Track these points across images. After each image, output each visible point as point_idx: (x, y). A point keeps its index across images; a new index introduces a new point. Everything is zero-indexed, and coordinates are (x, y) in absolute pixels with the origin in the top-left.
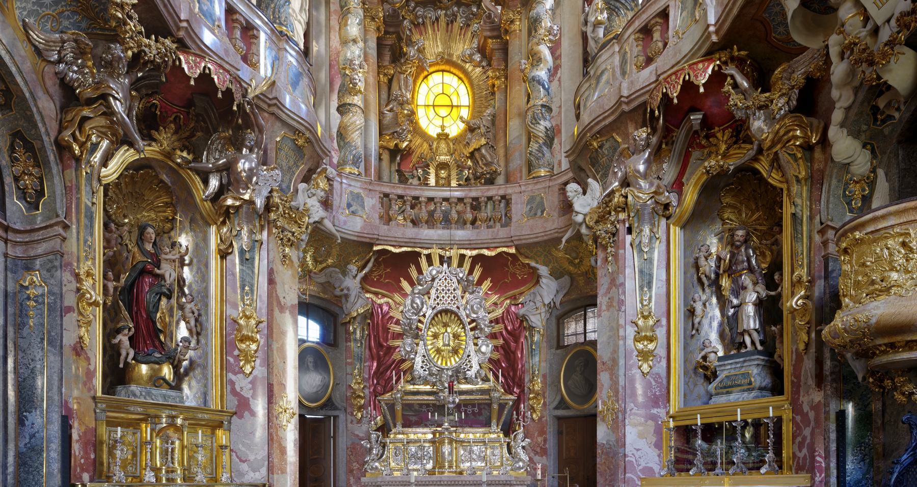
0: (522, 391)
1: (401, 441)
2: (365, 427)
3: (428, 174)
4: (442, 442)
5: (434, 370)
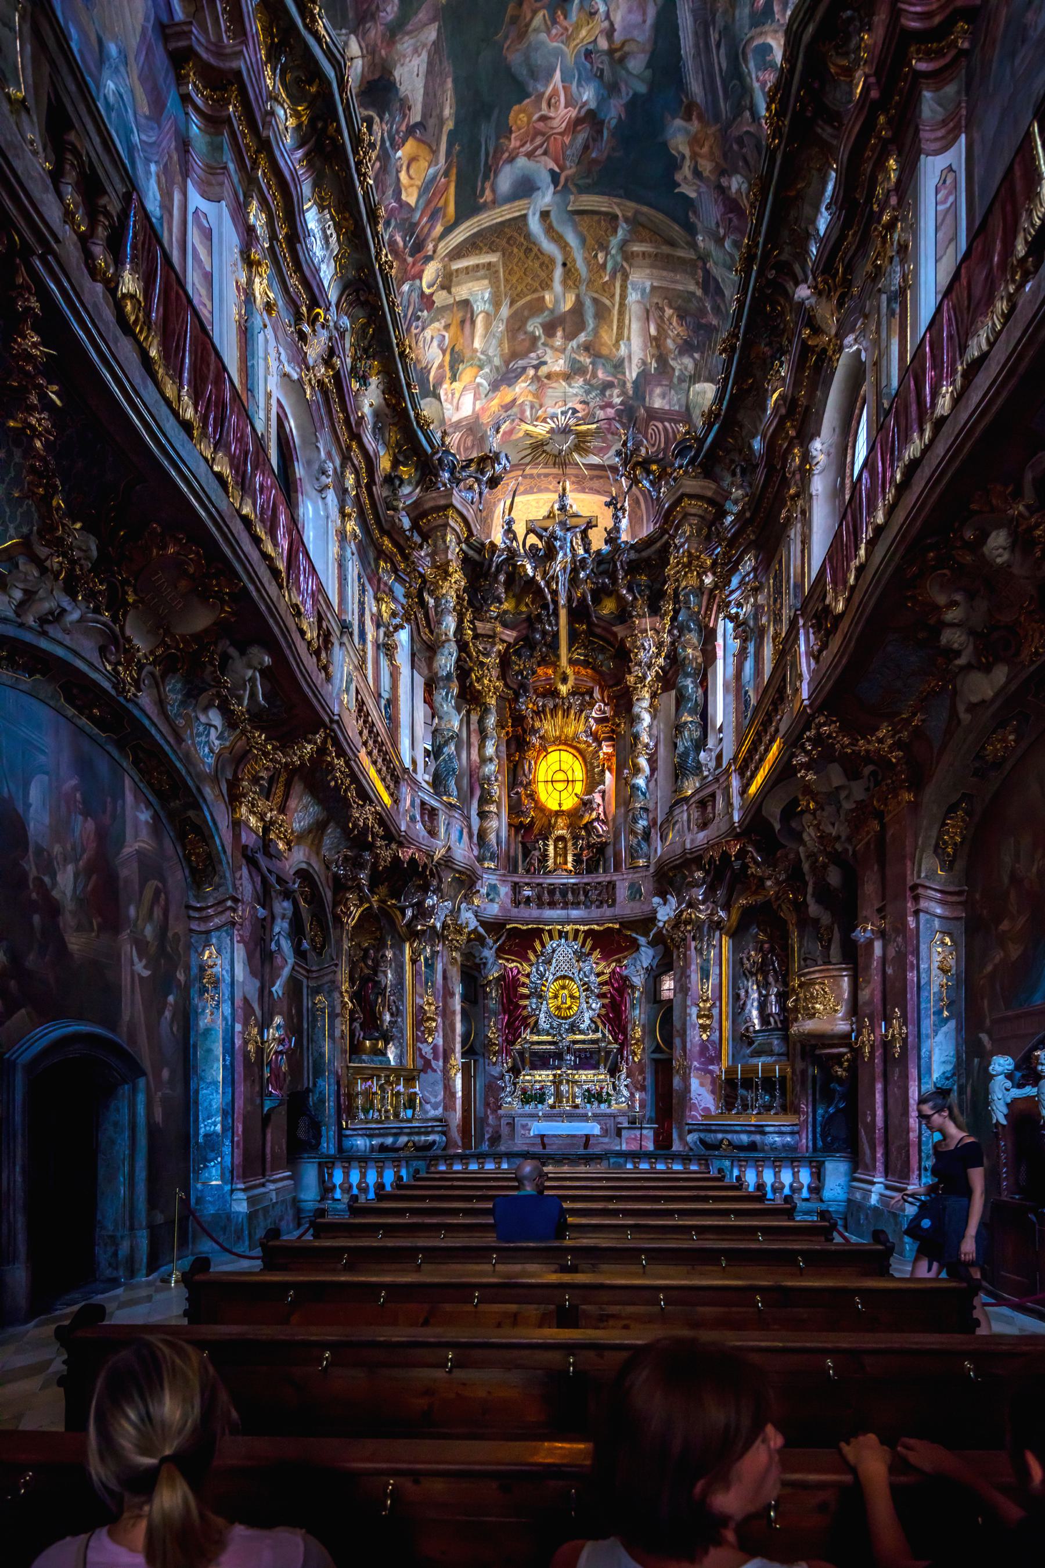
2: (498, 1069)
4: (561, 1082)
5: (555, 1024)
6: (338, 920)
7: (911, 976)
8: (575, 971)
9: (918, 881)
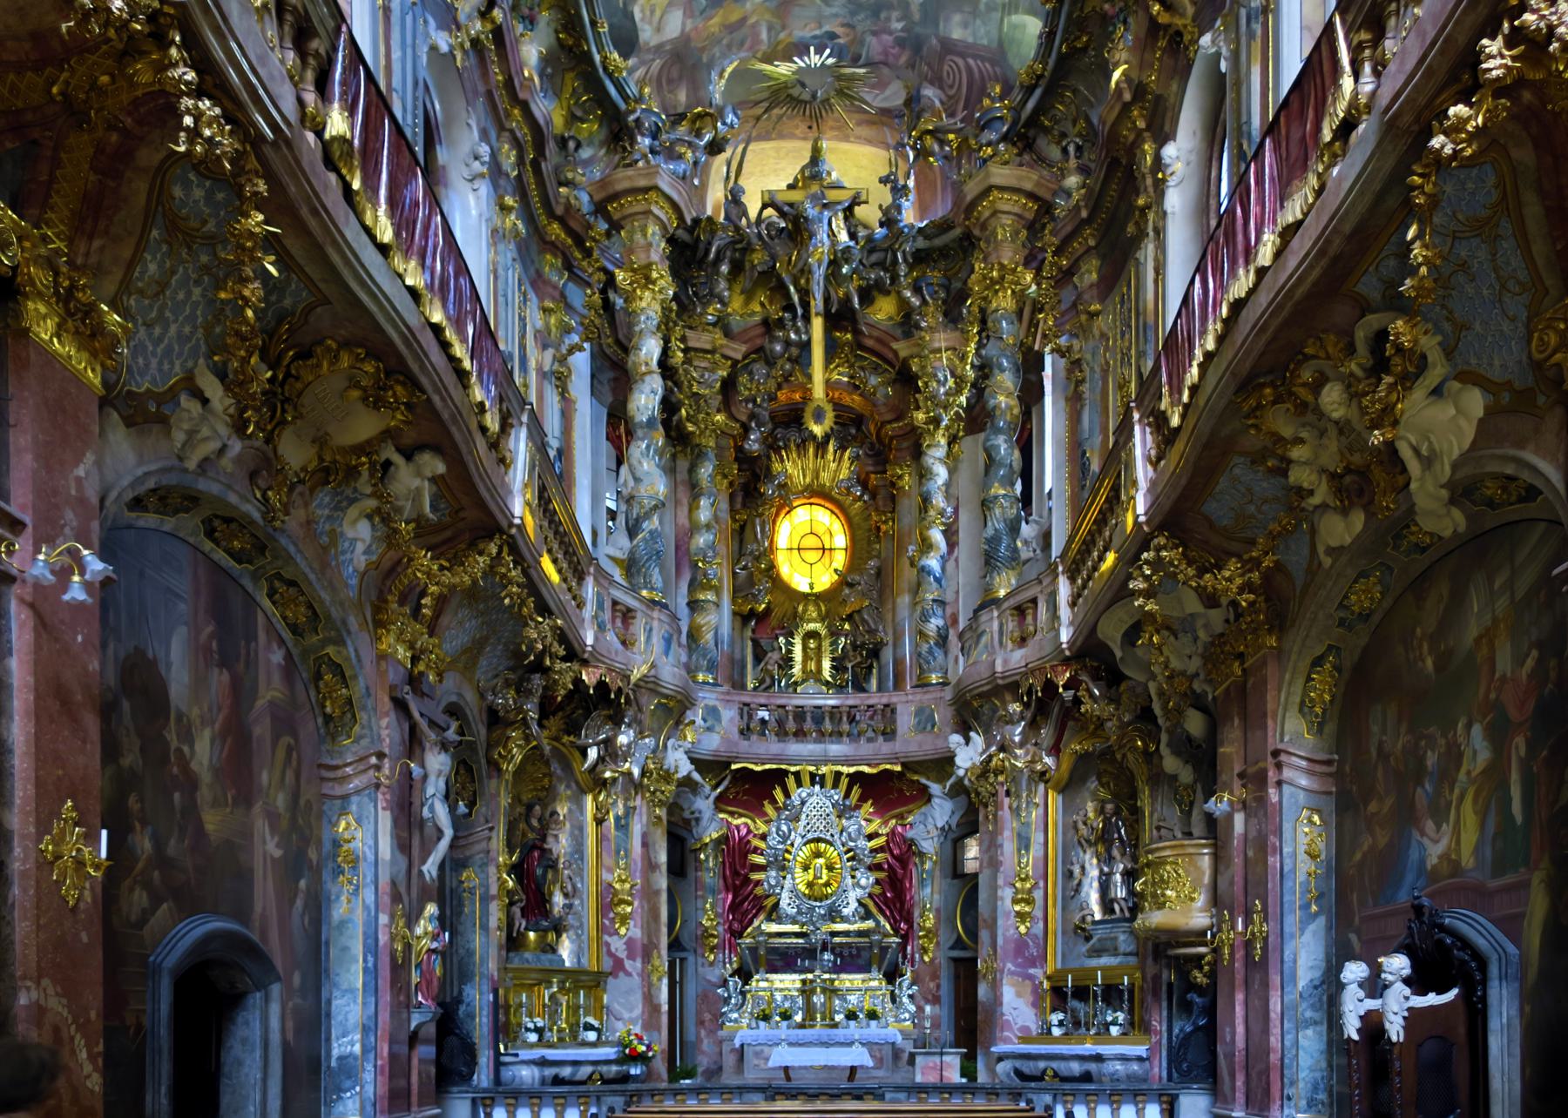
0: (911, 926)
1: (764, 990)
3: (792, 644)
4: (813, 992)
6: (495, 767)
7: (1273, 861)
8: (835, 831)
9: (1280, 746)
